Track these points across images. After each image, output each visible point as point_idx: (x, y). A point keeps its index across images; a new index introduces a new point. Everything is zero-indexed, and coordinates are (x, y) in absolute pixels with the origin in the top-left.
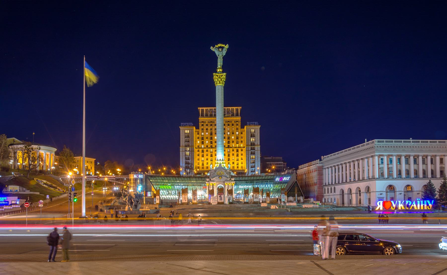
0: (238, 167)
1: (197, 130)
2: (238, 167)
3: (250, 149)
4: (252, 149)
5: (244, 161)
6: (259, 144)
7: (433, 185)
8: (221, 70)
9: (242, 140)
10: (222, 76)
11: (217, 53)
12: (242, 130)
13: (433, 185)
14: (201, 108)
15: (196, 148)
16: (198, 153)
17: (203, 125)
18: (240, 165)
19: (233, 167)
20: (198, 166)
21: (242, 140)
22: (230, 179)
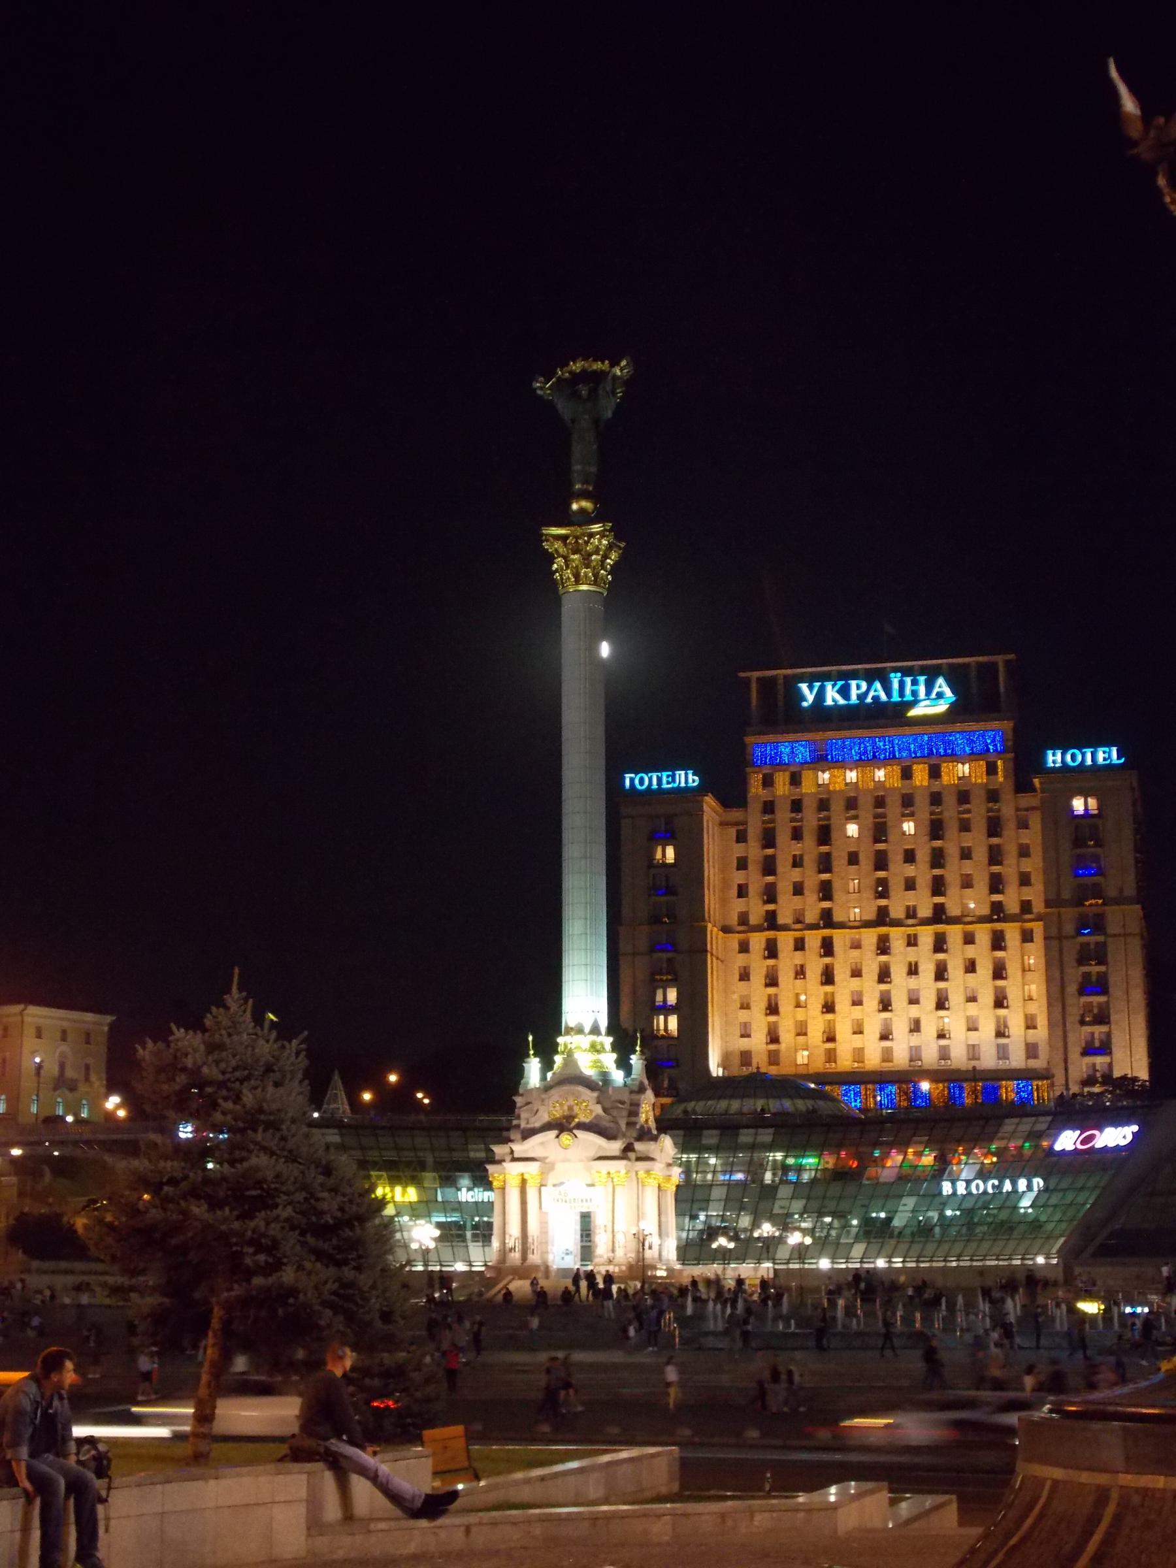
0: (1003, 1053)
1: (736, 815)
2: (1003, 1053)
3: (1069, 928)
4: (1082, 923)
6: (1130, 890)
8: (586, 504)
9: (1027, 865)
10: (591, 535)
11: (564, 407)
12: (1026, 800)
14: (756, 674)
15: (726, 930)
16: (741, 960)
17: (768, 782)
20: (744, 1044)
21: (1027, 865)
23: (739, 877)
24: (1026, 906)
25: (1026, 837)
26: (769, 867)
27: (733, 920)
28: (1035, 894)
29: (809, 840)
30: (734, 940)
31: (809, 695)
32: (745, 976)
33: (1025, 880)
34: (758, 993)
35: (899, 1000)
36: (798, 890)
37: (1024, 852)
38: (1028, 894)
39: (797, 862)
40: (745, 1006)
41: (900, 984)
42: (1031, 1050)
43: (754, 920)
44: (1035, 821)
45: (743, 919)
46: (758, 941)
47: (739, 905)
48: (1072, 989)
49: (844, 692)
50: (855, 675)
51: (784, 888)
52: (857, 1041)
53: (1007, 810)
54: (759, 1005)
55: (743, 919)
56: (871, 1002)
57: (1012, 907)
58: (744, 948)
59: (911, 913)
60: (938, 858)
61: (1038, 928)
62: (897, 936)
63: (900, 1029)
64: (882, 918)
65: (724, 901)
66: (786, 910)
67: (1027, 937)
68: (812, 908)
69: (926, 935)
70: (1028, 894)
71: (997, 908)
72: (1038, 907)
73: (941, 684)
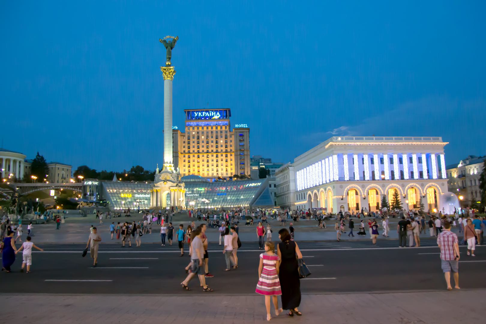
0: (227, 174)
2: (227, 174)
5: (233, 167)
7: (133, 167)
9: (231, 144)
13: (133, 167)
15: (181, 153)
18: (229, 171)
19: (213, 174)
21: (231, 144)
22: (177, 185)
23: (184, 145)
24: (231, 150)
25: (231, 139)
26: (189, 143)
27: (183, 152)
28: (233, 149)
29: (196, 139)
30: (183, 155)
31: (196, 115)
32: (185, 161)
33: (231, 146)
34: (187, 164)
35: (210, 165)
36: (194, 147)
37: (231, 141)
38: (231, 148)
39: (194, 142)
40: (185, 166)
41: (210, 163)
42: (231, 174)
43: (186, 151)
44: (233, 136)
45: (184, 152)
46: (187, 155)
47: (184, 149)
48: (239, 163)
49: (202, 114)
50: (204, 111)
51: (191, 147)
52: (203, 172)
53: (228, 134)
54: (187, 166)
55: (184, 152)
56: (206, 166)
57: (229, 150)
58: (184, 157)
59: (203, 151)
60: (208, 143)
61: (233, 154)
62: (210, 155)
63: (210, 170)
64: (208, 152)
65: (181, 148)
66: (191, 150)
67: (231, 155)
68: (196, 150)
69: (205, 155)
70: (231, 148)
71: (226, 150)
72: (233, 150)
73: (218, 113)
